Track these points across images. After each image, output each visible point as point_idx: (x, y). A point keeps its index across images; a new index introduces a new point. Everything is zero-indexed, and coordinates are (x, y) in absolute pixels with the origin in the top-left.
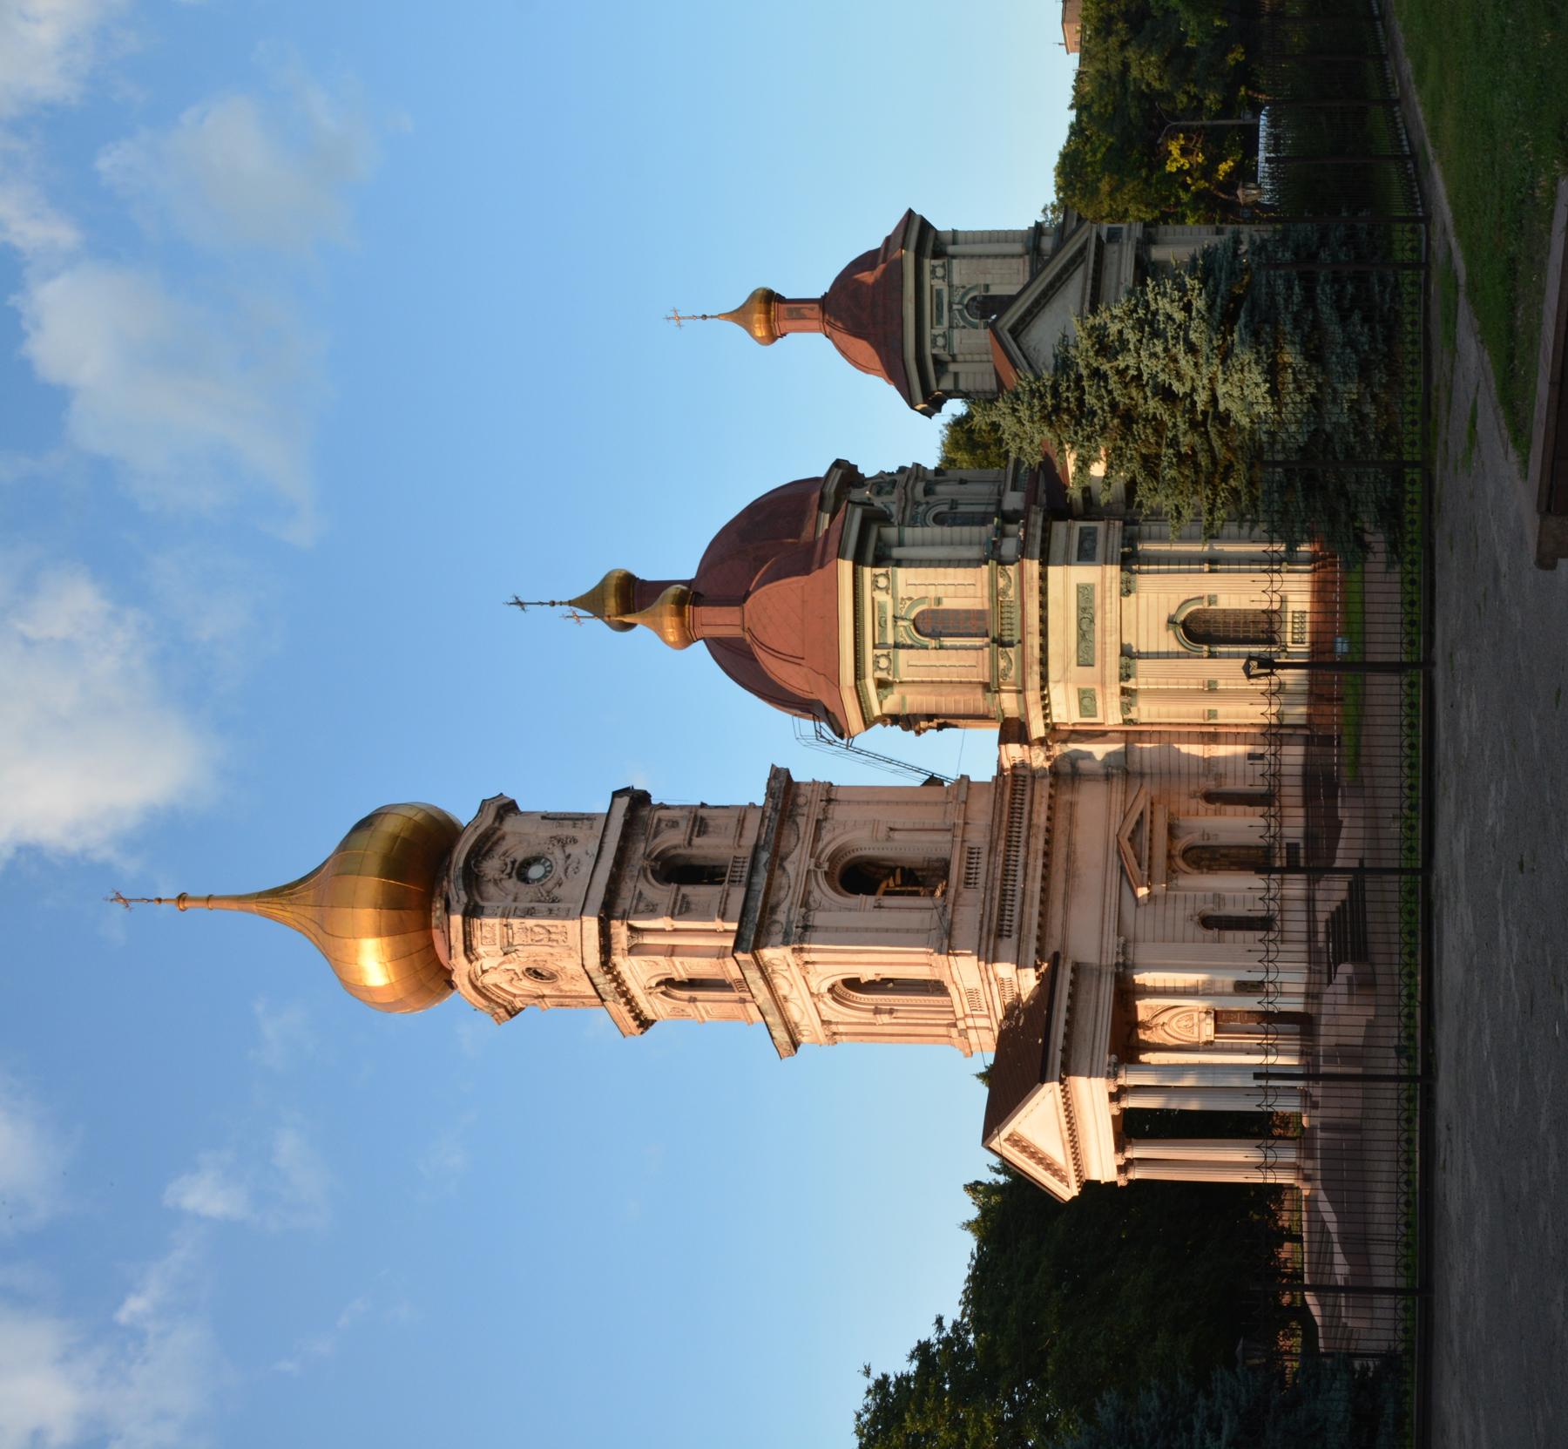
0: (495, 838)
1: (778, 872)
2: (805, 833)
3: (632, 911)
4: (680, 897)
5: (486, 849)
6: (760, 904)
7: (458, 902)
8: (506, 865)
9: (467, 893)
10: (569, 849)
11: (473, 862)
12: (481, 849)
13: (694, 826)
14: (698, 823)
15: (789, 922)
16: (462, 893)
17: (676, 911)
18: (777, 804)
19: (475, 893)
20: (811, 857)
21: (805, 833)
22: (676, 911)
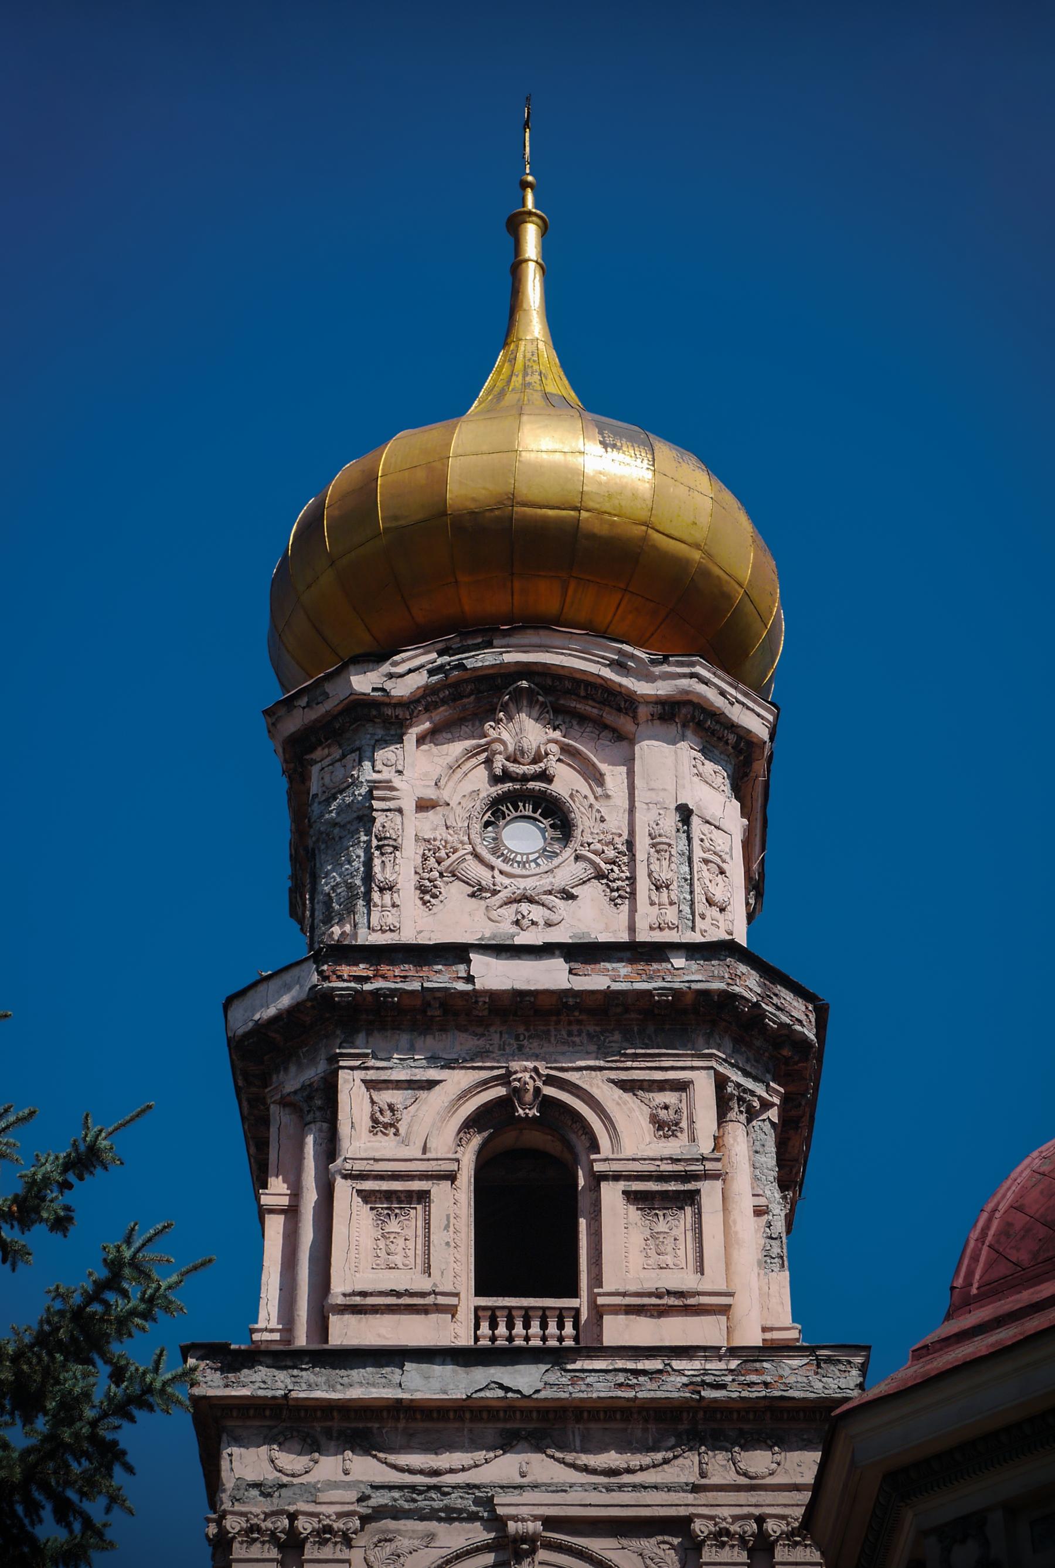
0: (610, 717)
1: (490, 1431)
2: (636, 1487)
3: (371, 1075)
4: (416, 1185)
5: (581, 707)
6: (355, 1393)
7: (391, 676)
8: (535, 761)
9: (428, 690)
10: (592, 894)
11: (524, 684)
12: (568, 692)
13: (662, 1177)
14: (672, 1186)
15: (311, 1492)
16: (420, 679)
17: (368, 1185)
18: (723, 1386)
19: (442, 713)
20: (550, 1523)
21: (636, 1487)
22: (368, 1185)
